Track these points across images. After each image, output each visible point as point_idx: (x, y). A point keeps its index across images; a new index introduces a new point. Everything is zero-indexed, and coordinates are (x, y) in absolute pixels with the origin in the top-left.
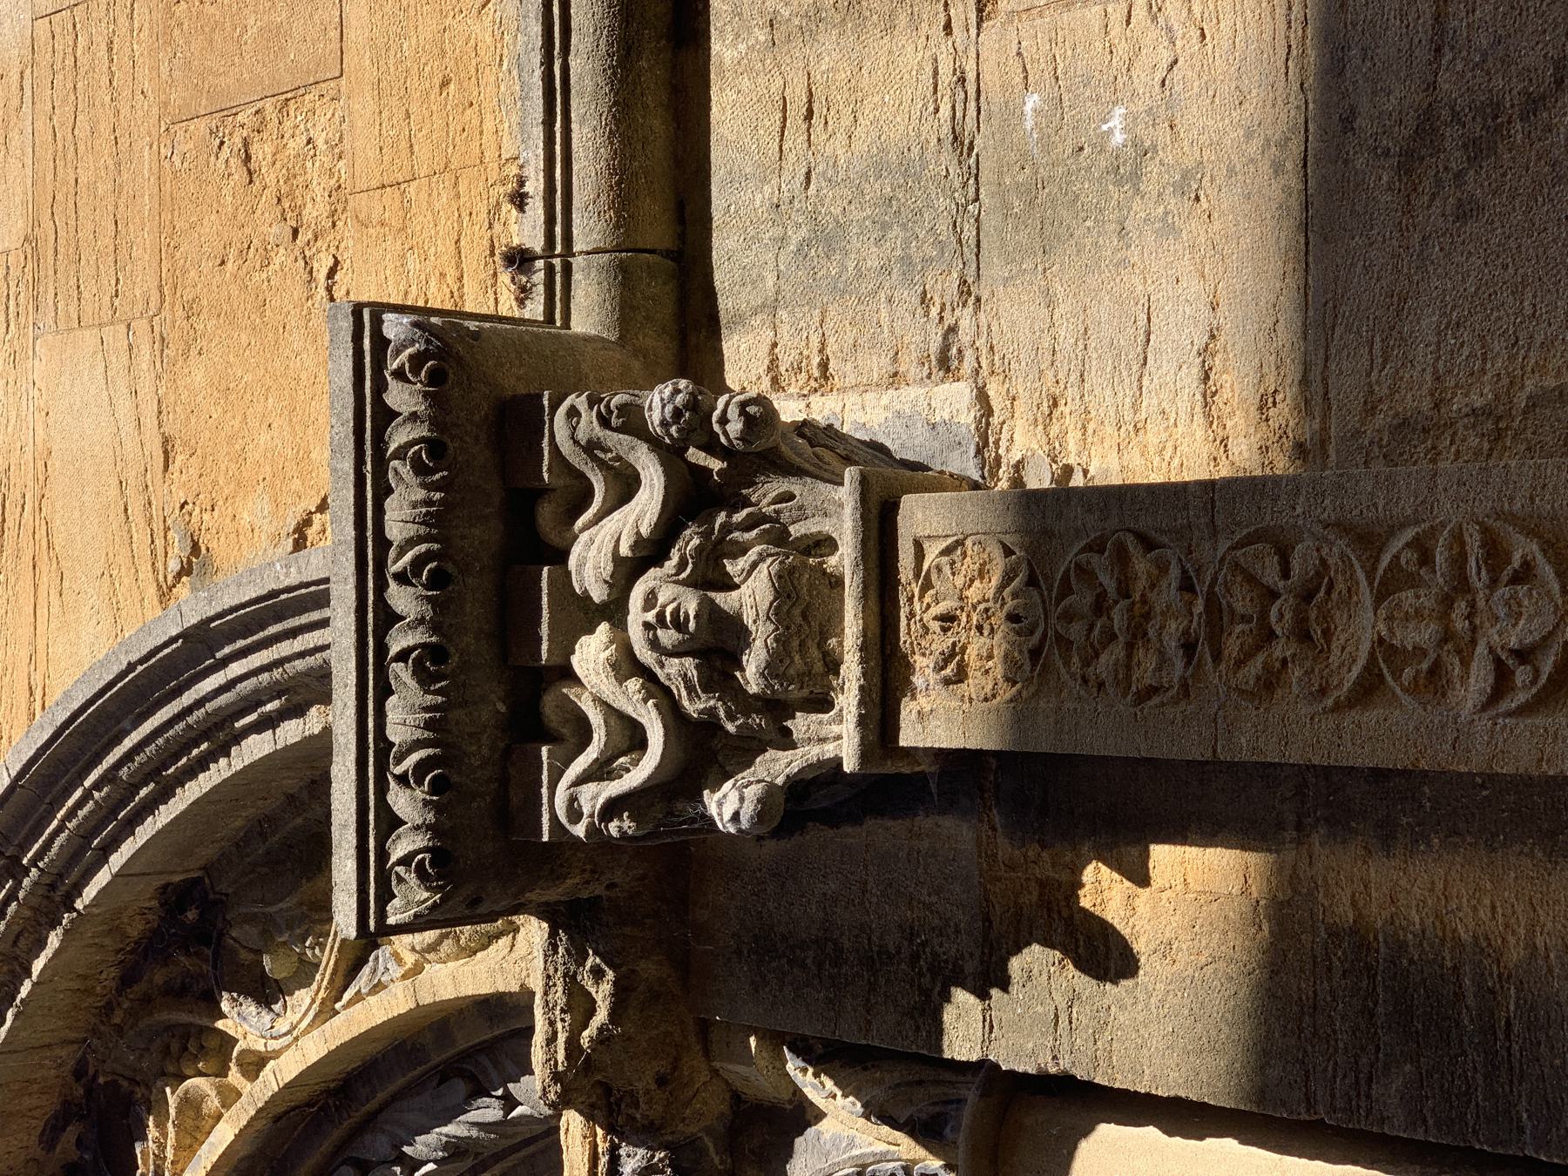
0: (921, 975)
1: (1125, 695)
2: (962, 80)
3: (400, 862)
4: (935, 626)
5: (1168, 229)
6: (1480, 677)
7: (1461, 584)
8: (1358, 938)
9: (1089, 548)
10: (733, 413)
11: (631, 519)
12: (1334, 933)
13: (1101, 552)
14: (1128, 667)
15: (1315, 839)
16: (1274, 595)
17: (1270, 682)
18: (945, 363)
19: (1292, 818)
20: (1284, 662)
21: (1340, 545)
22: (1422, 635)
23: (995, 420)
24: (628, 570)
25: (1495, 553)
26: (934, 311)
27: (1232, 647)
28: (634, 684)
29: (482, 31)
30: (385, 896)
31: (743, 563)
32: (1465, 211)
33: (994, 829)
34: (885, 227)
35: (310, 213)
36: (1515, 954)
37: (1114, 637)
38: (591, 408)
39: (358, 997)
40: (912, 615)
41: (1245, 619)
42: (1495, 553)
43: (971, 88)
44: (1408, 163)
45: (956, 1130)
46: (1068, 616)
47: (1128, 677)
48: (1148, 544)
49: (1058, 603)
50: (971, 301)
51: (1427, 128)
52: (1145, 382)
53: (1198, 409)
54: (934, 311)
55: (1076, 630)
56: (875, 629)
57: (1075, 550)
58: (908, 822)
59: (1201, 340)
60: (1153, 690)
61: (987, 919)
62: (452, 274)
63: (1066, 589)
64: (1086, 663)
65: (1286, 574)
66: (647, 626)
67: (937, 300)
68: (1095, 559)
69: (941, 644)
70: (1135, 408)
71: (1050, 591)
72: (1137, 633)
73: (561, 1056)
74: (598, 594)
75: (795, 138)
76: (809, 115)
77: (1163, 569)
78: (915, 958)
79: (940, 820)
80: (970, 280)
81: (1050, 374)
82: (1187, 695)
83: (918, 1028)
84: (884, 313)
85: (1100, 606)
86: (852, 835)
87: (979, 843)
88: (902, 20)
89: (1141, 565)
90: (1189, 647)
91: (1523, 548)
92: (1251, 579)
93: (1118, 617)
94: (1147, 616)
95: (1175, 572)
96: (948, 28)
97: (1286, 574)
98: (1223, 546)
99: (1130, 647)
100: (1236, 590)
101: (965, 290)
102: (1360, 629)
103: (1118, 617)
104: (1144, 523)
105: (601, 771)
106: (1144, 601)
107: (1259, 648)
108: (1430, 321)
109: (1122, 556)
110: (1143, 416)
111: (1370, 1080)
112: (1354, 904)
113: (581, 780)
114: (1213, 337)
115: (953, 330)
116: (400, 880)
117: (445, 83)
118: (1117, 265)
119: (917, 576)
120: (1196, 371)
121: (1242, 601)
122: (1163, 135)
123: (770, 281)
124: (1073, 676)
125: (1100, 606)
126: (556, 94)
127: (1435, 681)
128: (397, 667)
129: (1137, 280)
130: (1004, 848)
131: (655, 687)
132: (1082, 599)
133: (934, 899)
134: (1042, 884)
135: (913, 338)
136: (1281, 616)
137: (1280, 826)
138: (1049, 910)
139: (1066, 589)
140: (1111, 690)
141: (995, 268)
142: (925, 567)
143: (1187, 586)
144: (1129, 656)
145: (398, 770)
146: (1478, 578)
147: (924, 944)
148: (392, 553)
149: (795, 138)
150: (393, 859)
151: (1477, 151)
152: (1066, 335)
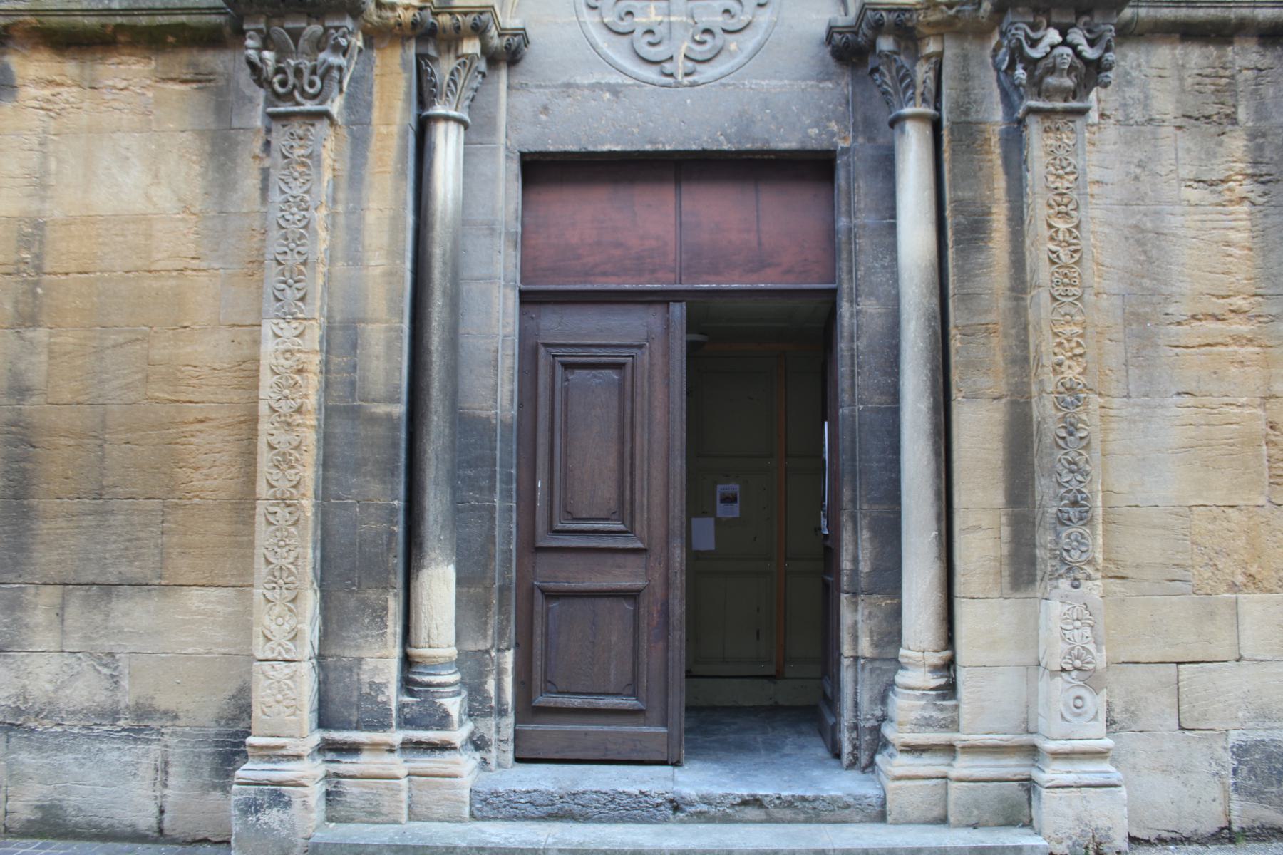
5: (1128, 174)
6: (1054, 248)
7: (1070, 244)
8: (990, 213)
17: (1050, 206)
18: (1102, 116)
21: (1076, 221)
22: (1061, 237)
24: (1074, 47)
25: (1075, 251)
27: (1058, 198)
28: (1048, 49)
32: (1126, 238)
36: (991, 245)
42: (1075, 251)
44: (1136, 227)
51: (1142, 231)
55: (1058, 162)
72: (1059, 176)
74: (1069, 38)
75: (1154, 72)
85: (1063, 168)
86: (995, 85)
89: (1071, 178)
91: (1077, 256)
93: (1061, 172)
102: (1061, 225)
103: (1061, 172)
108: (1107, 230)
109: (1073, 173)
121: (1065, 200)
127: (1052, 239)
130: (998, 128)
131: (1047, 54)
132: (1065, 163)
135: (1108, 106)
136: (1063, 208)
141: (1123, 129)
146: (1072, 248)
149: (1154, 72)
151: (1138, 241)
152: (1108, 148)
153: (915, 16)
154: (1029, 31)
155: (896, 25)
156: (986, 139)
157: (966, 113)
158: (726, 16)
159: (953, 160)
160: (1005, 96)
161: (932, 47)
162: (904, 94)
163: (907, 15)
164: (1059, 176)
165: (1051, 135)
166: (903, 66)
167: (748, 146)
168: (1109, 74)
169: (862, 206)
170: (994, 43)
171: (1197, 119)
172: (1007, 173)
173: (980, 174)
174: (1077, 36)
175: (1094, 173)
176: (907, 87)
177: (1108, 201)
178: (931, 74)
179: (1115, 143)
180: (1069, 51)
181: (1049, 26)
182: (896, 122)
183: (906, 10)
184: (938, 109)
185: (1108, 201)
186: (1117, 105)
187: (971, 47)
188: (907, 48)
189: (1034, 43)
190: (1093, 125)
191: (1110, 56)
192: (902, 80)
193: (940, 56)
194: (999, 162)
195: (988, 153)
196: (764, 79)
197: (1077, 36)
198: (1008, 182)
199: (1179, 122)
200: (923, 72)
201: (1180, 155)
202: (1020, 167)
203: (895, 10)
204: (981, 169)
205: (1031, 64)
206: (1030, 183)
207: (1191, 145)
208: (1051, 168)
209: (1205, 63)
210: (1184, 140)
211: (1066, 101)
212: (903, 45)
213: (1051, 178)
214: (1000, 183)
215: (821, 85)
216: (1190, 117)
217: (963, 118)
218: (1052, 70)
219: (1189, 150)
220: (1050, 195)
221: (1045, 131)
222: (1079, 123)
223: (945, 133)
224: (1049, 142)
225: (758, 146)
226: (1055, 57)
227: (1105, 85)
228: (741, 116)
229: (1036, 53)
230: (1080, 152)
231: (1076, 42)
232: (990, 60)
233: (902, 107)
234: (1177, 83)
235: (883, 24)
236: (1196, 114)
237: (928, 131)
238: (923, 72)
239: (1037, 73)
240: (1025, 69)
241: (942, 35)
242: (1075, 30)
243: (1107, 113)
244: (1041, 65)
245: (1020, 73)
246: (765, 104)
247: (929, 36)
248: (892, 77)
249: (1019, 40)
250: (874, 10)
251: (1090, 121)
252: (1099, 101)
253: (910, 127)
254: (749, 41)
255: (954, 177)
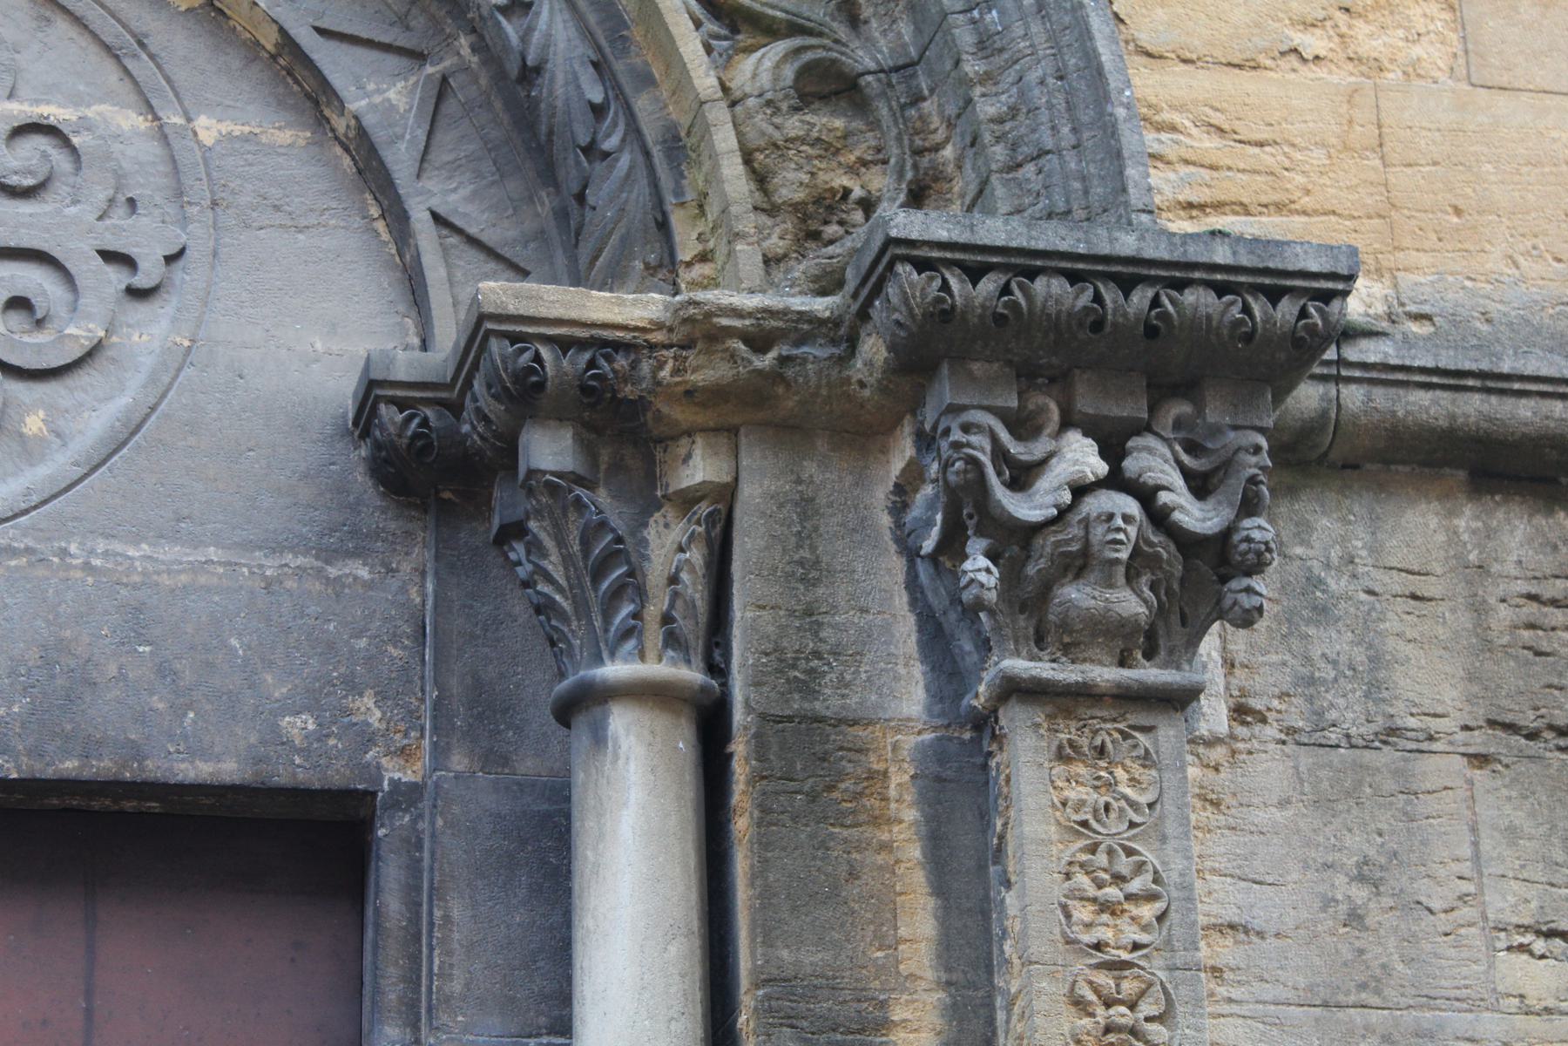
0: (807, 660)
1: (1066, 896)
2: (1431, 738)
3: (945, 281)
4: (1098, 742)
5: (1328, 902)
9: (1156, 872)
10: (1256, 601)
11: (1184, 503)
12: (883, 1005)
13: (1155, 881)
14: (1082, 899)
15: (941, 995)
16: (1132, 1006)
17: (1079, 1004)
18: (1241, 712)
19: (954, 978)
20: (1092, 1015)
23: (1201, 750)
24: (1146, 495)
26: (1275, 703)
27: (1105, 979)
28: (1067, 497)
29: (1494, 262)
30: (922, 265)
31: (1147, 593)
33: (919, 733)
34: (1335, 663)
35: (1361, 29)
37: (1100, 888)
38: (1261, 468)
39: (698, 24)
40: (1104, 720)
41: (1118, 985)
43: (1425, 746)
45: (674, 662)
46: (1110, 852)
47: (1075, 898)
48: (1161, 918)
49: (1121, 845)
50: (1283, 737)
52: (1229, 880)
53: (1213, 920)
54: (1275, 703)
55: (1102, 859)
56: (1096, 691)
57: (1156, 862)
58: (916, 655)
59: (1257, 924)
60: (1068, 916)
61: (855, 723)
62: (1306, 202)
63: (1130, 852)
64: (1082, 865)
65: (1147, 1019)
66: (1111, 517)
67: (1283, 707)
68: (1149, 877)
69: (1084, 742)
70: (1214, 871)
71: (1128, 839)
72: (1106, 907)
73: (725, 322)
74: (1131, 465)
75: (1397, 582)
76: (1414, 597)
77: (1145, 928)
78: (817, 655)
79: (921, 684)
80: (1296, 736)
81: (1234, 803)
82: (1067, 943)
83: (767, 654)
84: (1274, 658)
85: (1119, 879)
86: (901, 600)
87: (909, 719)
88: (1475, 689)
89: (1147, 912)
90: (1098, 946)
92: (1142, 994)
93: (1112, 892)
94: (1113, 913)
95: (1143, 938)
96: (1466, 728)
97: (1147, 1019)
98: (1162, 975)
99: (1094, 900)
100: (1136, 984)
101: (1291, 731)
103: (1112, 892)
104: (1174, 916)
105: (1000, 455)
106: (1123, 911)
107: (1100, 997)
109: (1152, 897)
110: (1208, 877)
111: (792, 1026)
112: (905, 1021)
113: (995, 439)
114: (1258, 933)
115: (1264, 721)
116: (931, 279)
117: (1458, 211)
118: (1305, 861)
119: (1130, 727)
120: (1236, 919)
121: (1129, 987)
122: (1388, 901)
123: (1299, 550)
124: (1074, 855)
125: (1119, 879)
126: (1453, 380)
128: (1090, 292)
129: (1295, 876)
130: (909, 741)
131: (1063, 513)
132: (1124, 865)
133: (864, 676)
134: (885, 773)
135: (1258, 682)
136: (1120, 1014)
137: (949, 969)
138: (867, 779)
139: (1130, 852)
140: (1067, 884)
141: (1306, 758)
142: (1137, 734)
143: (1136, 946)
144: (1088, 899)
145: (1014, 286)
147: (829, 664)
148: (1174, 293)
149: (1397, 582)
150: (948, 275)
152: (1260, 817)
153: (646, 367)
154: (1004, 436)
155: (585, 389)
156: (871, 775)
157: (807, 688)
158: (16, 319)
159: (763, 844)
160: (935, 639)
161: (699, 468)
162: (607, 617)
163: (622, 362)
164: (1106, 907)
165: (1080, 769)
166: (603, 525)
167: (69, 766)
168: (1257, 583)
169: (457, 986)
170: (897, 466)
171: (1532, 736)
172: (940, 889)
173: (853, 890)
174: (1155, 461)
175: (1219, 899)
176: (617, 593)
177: (1269, 991)
178: (696, 555)
179: (1284, 803)
180: (1132, 506)
181: (1066, 424)
182: (580, 706)
183: (617, 346)
184: (717, 669)
185: (1269, 991)
186: (1286, 682)
187: (824, 474)
188: (617, 467)
189: (1022, 476)
190: (1213, 742)
191: (1258, 528)
192: (598, 574)
193: (727, 494)
194: (915, 852)
195: (877, 821)
196: (136, 540)
197: (1155, 461)
198: (945, 917)
199: (1479, 741)
200: (668, 547)
201: (1486, 846)
202: (982, 868)
203: (582, 344)
204: (853, 875)
205: (1014, 541)
206: (1015, 926)
207: (1519, 817)
208: (1082, 880)
209: (1547, 563)
210: (1497, 801)
211: (1122, 663)
212: (605, 456)
213: (1083, 913)
214: (919, 922)
215: (333, 572)
216: (1511, 728)
217: (797, 704)
218: (1079, 564)
219: (1512, 833)
220: (1080, 966)
221: (1061, 757)
222: (1167, 734)
223: (739, 748)
224: (1073, 794)
225: (103, 766)
226: (1086, 523)
227: (1247, 619)
228: (47, 663)
229: (1028, 508)
230: (1171, 828)
231: (1150, 478)
232: (886, 520)
233: (598, 660)
234: (1465, 620)
235: (540, 386)
236: (1528, 720)
237: (683, 740)
238: (668, 547)
239: (1031, 570)
240: (992, 555)
241: (733, 431)
242: (1150, 441)
243: (1256, 703)
244: (1046, 544)
245: (978, 566)
246: (136, 623)
247: (689, 433)
248: (567, 560)
249: (974, 462)
250: (514, 338)
251: (1203, 729)
252: (1230, 664)
253: (627, 728)
254: (93, 410)
255: (766, 897)
